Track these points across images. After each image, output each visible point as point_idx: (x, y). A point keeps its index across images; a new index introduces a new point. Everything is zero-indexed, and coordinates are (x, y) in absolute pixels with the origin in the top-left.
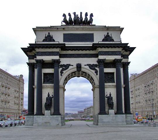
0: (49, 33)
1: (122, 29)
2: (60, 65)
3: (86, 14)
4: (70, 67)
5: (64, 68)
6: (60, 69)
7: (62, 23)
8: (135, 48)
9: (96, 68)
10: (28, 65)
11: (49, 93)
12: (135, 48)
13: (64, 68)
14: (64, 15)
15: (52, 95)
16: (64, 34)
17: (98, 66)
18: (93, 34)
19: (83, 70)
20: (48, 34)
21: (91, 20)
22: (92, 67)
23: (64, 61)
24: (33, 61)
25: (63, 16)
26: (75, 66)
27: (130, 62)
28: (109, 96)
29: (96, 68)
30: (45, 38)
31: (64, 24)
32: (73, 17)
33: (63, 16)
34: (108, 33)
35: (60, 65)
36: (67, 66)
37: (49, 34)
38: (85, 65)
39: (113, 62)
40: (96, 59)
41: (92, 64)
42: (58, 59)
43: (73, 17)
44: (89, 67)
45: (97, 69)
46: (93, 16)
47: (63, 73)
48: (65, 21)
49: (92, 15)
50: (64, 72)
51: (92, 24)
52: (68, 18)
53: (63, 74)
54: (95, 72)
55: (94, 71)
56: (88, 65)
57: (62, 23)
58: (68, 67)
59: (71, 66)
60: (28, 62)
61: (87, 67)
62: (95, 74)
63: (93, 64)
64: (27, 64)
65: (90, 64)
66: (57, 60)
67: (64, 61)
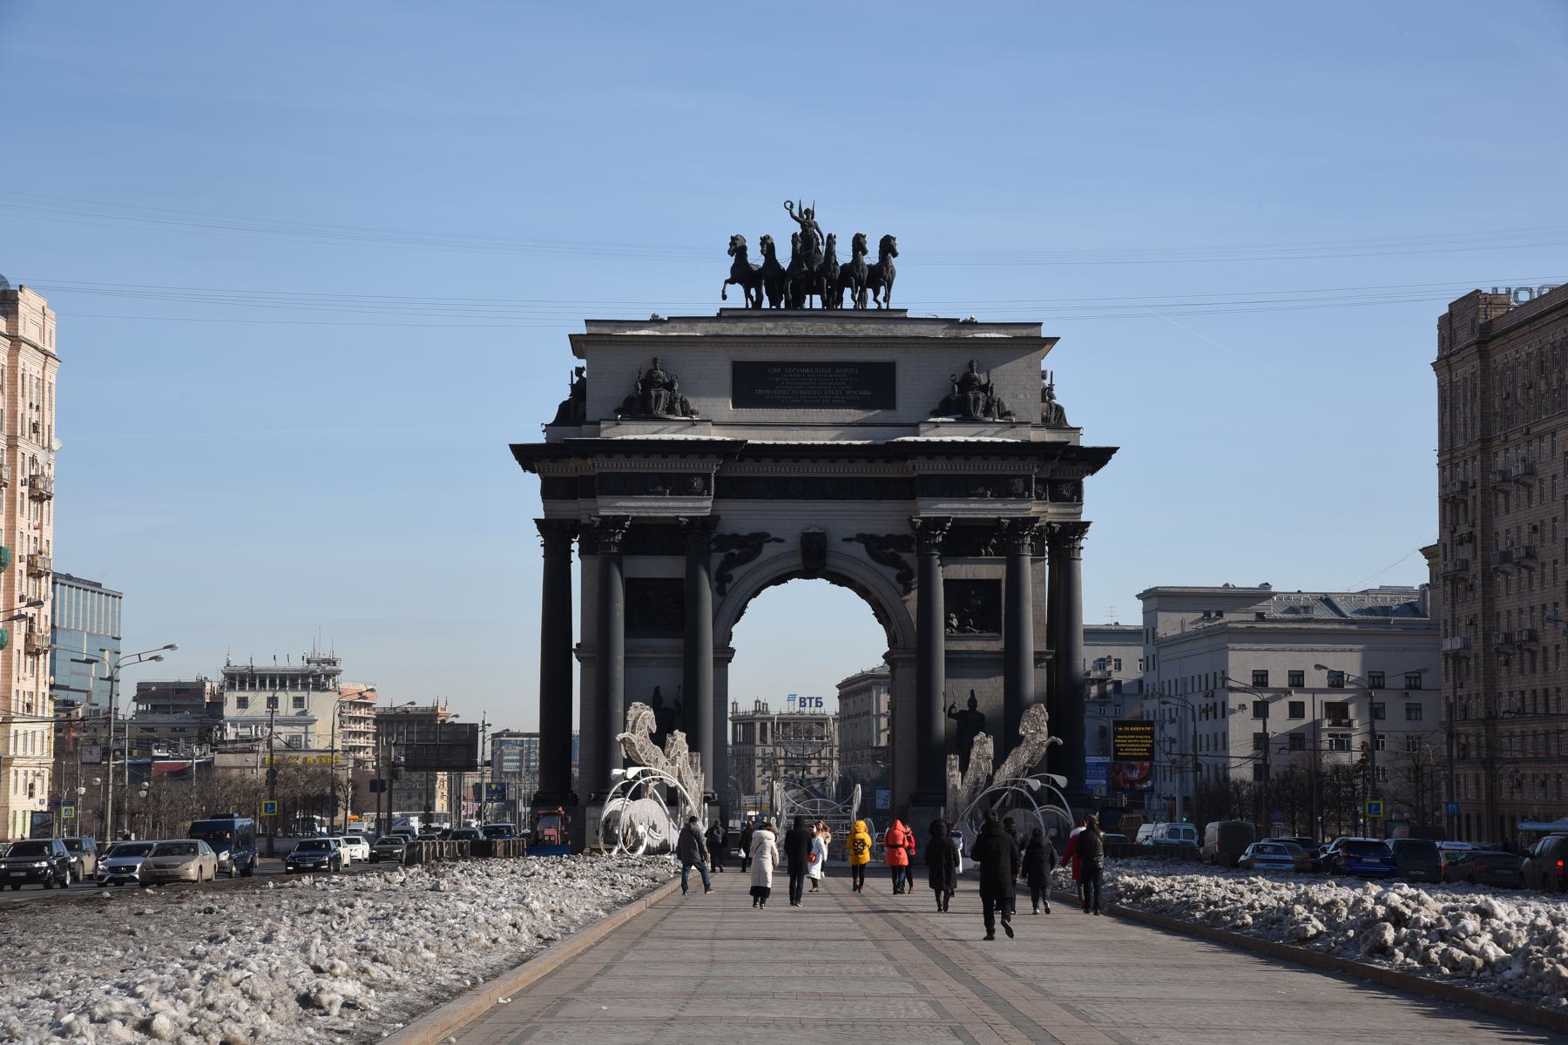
3: (859, 244)
4: (769, 550)
5: (736, 552)
6: (717, 559)
7: (724, 297)
8: (1118, 448)
9: (905, 556)
11: (657, 690)
12: (1114, 450)
13: (736, 552)
14: (738, 249)
15: (676, 702)
17: (914, 547)
19: (834, 563)
21: (880, 276)
22: (880, 547)
23: (743, 516)
24: (570, 509)
26: (792, 543)
27: (1087, 524)
28: (967, 709)
29: (905, 556)
31: (737, 297)
32: (784, 257)
33: (731, 253)
36: (751, 545)
38: (845, 540)
41: (883, 534)
42: (707, 512)
43: (784, 257)
44: (869, 550)
45: (910, 558)
46: (895, 255)
47: (730, 578)
48: (742, 273)
49: (888, 246)
50: (737, 573)
51: (886, 299)
52: (756, 258)
53: (728, 586)
54: (899, 578)
55: (891, 573)
56: (861, 538)
57: (724, 297)
58: (758, 550)
60: (542, 516)
61: (859, 550)
62: (900, 587)
63: (889, 536)
64: (535, 525)
67: (743, 516)
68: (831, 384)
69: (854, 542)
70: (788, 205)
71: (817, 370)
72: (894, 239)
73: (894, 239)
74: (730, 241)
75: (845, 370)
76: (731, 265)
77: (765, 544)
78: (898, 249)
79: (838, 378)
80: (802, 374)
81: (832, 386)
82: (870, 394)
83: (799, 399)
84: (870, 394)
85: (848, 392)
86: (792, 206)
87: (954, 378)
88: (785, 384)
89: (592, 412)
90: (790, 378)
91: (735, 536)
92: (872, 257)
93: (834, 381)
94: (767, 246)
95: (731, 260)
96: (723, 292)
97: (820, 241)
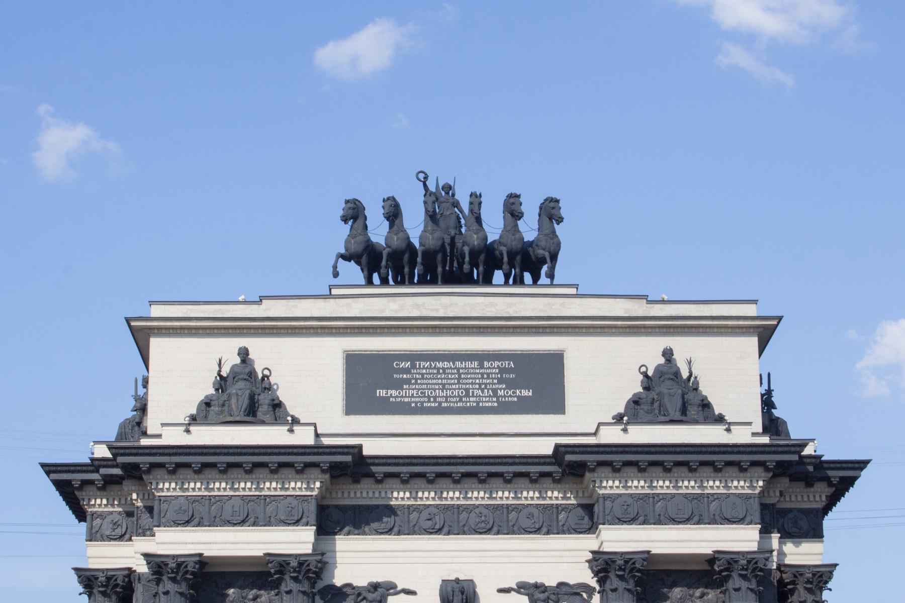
0: (244, 354)
1: (775, 322)
2: (320, 585)
7: (336, 275)
10: (81, 589)
12: (861, 465)
16: (353, 361)
18: (556, 361)
20: (238, 360)
25: (345, 219)
30: (212, 391)
34: (668, 354)
35: (320, 585)
37: (244, 361)
39: (706, 567)
40: (586, 544)
41: (551, 582)
46: (560, 220)
56: (522, 588)
57: (336, 275)
59: (402, 595)
63: (561, 584)
65: (536, 586)
66: (302, 562)
68: (477, 381)
69: (513, 593)
70: (421, 176)
71: (458, 364)
72: (557, 201)
73: (557, 201)
74: (343, 205)
75: (496, 364)
76: (346, 237)
77: (390, 598)
78: (563, 213)
79: (488, 374)
80: (438, 369)
81: (480, 384)
82: (530, 394)
83: (435, 401)
84: (530, 394)
85: (500, 393)
86: (426, 178)
87: (643, 369)
88: (416, 383)
89: (152, 424)
90: (423, 374)
91: (349, 585)
92: (529, 229)
93: (483, 378)
94: (393, 214)
95: (346, 229)
96: (335, 267)
97: (463, 221)
